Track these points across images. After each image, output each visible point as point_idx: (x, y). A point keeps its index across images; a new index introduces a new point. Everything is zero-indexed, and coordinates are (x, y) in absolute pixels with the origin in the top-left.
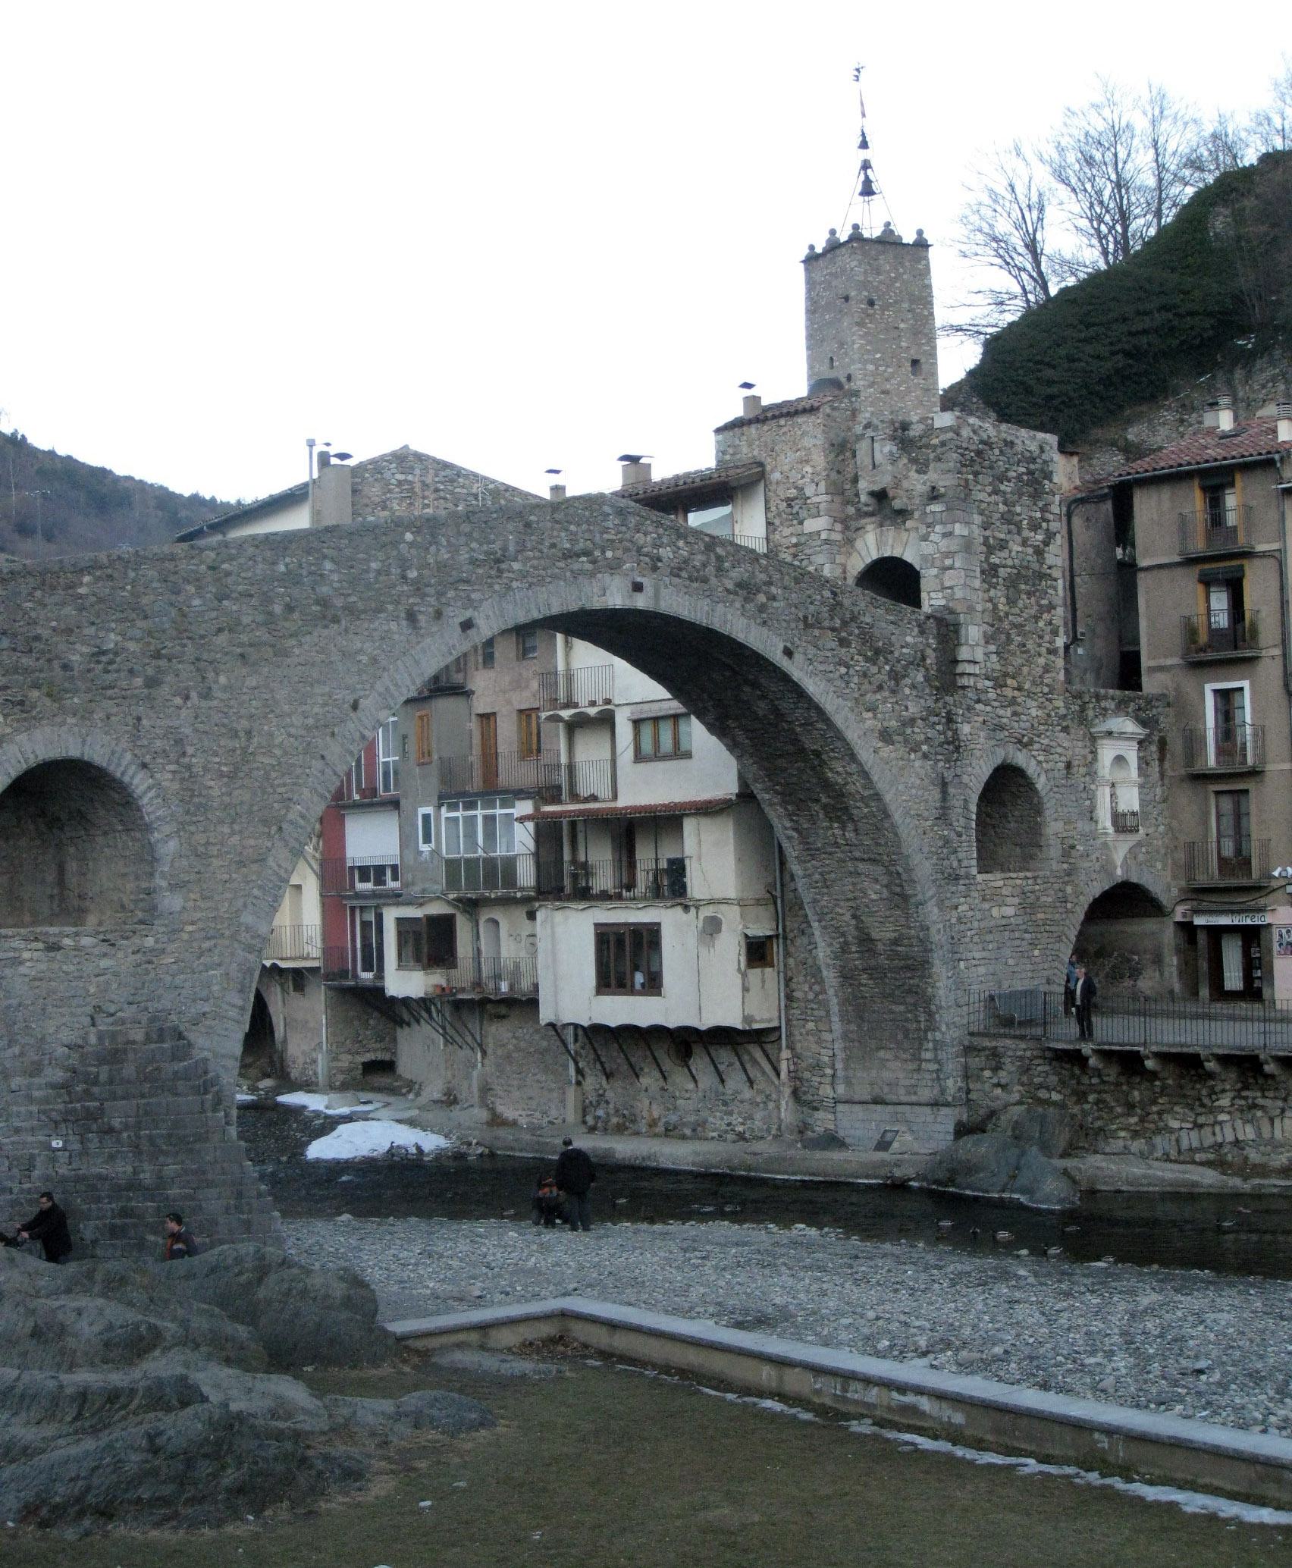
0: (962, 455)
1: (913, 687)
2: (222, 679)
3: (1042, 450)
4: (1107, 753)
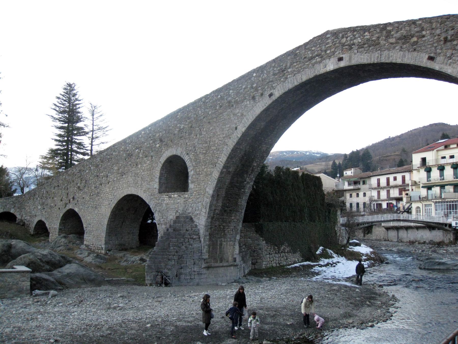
2: (204, 130)
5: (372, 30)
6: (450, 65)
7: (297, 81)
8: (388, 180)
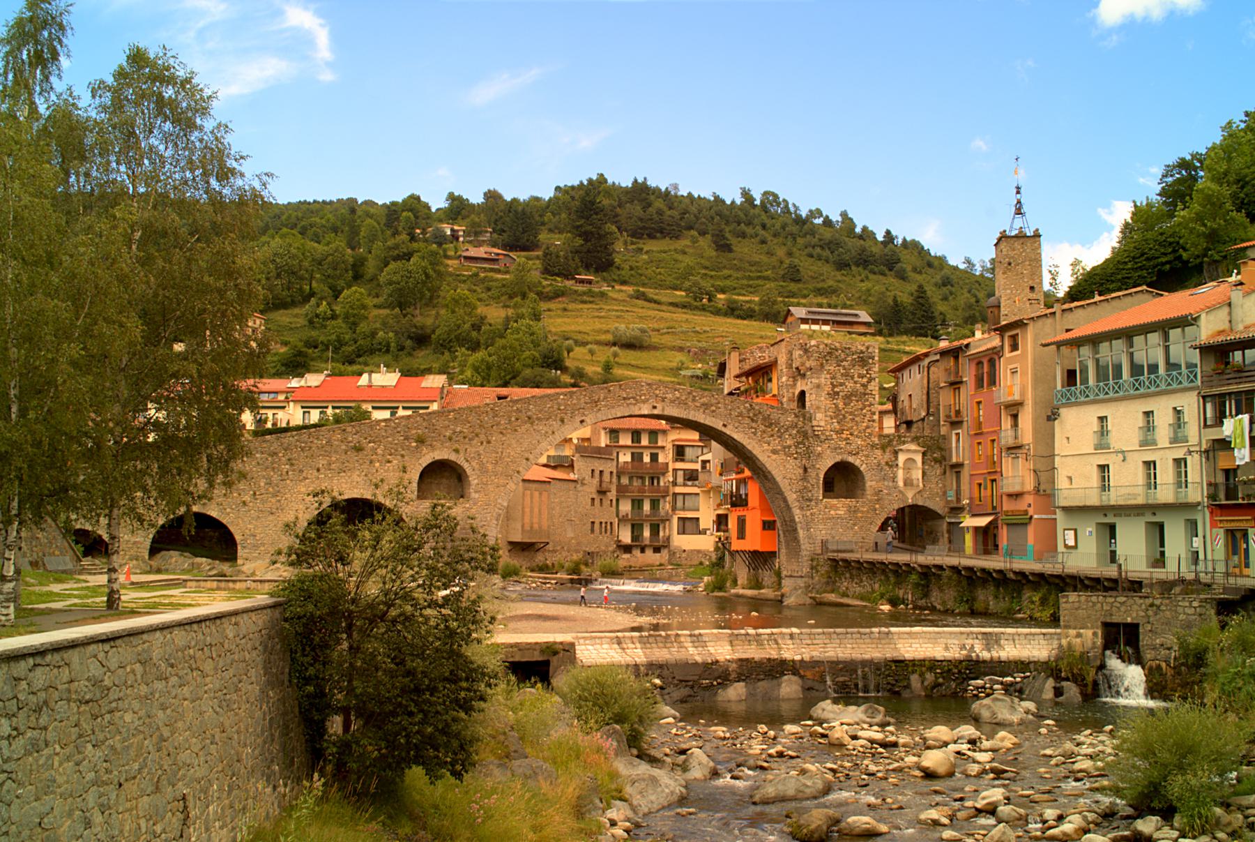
3: (868, 348)
4: (902, 458)
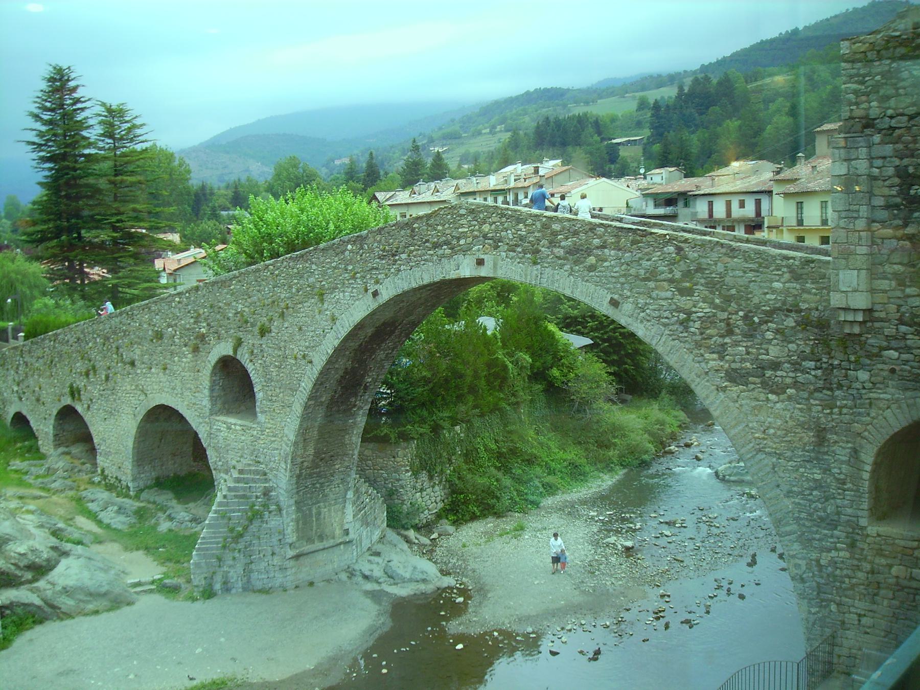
0: (862, 83)
1: (777, 331)
5: (529, 221)
6: (641, 322)
7: (415, 279)
8: (729, 204)
